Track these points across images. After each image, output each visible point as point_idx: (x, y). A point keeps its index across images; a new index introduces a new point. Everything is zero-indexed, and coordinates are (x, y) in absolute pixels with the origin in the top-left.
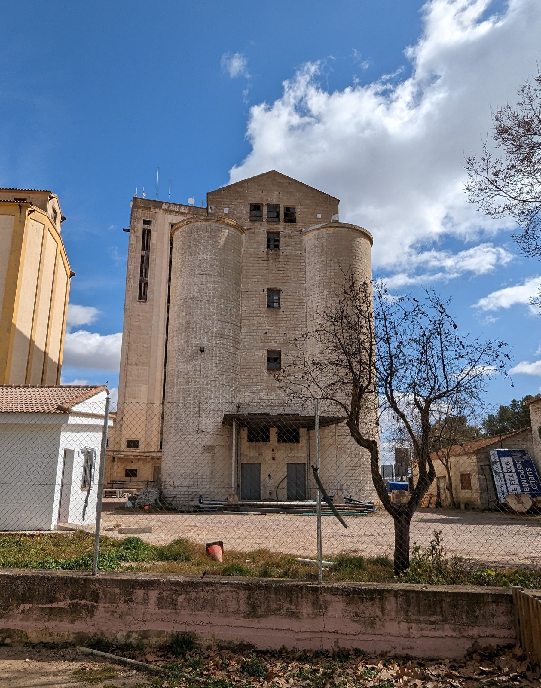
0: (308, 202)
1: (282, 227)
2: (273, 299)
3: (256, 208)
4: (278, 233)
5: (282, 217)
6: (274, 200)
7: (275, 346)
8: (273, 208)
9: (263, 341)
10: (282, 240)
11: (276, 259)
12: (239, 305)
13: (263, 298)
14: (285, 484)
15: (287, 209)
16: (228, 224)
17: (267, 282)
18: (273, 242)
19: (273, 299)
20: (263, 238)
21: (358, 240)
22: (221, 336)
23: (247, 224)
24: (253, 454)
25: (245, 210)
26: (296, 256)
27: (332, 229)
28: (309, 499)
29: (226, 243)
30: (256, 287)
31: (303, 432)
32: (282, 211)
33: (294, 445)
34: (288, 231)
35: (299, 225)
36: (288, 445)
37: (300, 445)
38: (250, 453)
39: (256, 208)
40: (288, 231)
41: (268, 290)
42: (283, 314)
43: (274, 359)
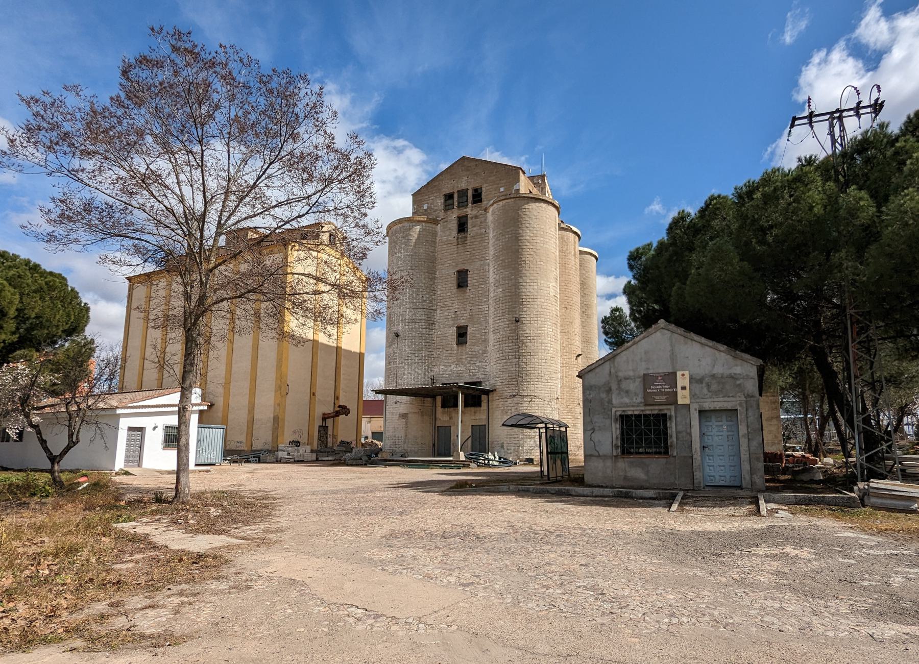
0: (493, 178)
1: (470, 211)
2: (462, 280)
3: (449, 197)
4: (467, 216)
5: (470, 199)
6: (463, 185)
7: (462, 322)
8: (463, 193)
9: (453, 319)
10: (470, 222)
11: (464, 243)
12: (433, 291)
13: (453, 280)
14: (469, 441)
15: (476, 190)
16: (419, 221)
17: (457, 265)
18: (462, 226)
19: (462, 280)
20: (454, 225)
21: (527, 206)
22: (413, 321)
23: (442, 214)
24: (446, 418)
25: (440, 202)
26: (481, 234)
27: (501, 203)
28: (450, 456)
29: (418, 238)
30: (447, 273)
31: (484, 397)
32: (470, 193)
33: (478, 409)
34: (475, 212)
35: (484, 203)
36: (472, 409)
37: (482, 408)
38: (442, 417)
39: (449, 197)
40: (475, 212)
41: (458, 272)
42: (470, 291)
43: (462, 335)
